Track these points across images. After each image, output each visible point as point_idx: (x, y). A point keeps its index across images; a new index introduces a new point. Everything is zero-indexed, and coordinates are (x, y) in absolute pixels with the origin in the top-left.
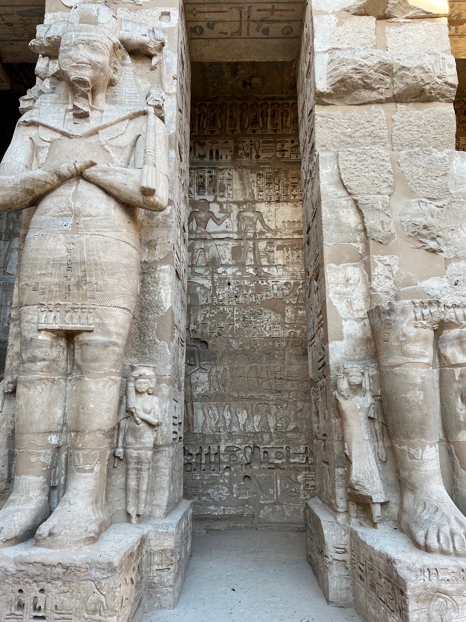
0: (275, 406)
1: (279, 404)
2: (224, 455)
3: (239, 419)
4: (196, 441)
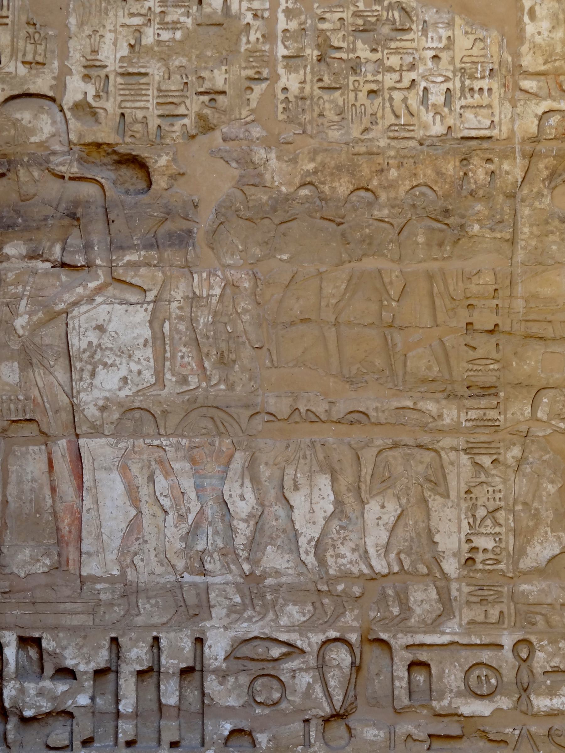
0: (464, 459)
1: (487, 447)
2: (223, 676)
3: (297, 515)
4: (93, 613)
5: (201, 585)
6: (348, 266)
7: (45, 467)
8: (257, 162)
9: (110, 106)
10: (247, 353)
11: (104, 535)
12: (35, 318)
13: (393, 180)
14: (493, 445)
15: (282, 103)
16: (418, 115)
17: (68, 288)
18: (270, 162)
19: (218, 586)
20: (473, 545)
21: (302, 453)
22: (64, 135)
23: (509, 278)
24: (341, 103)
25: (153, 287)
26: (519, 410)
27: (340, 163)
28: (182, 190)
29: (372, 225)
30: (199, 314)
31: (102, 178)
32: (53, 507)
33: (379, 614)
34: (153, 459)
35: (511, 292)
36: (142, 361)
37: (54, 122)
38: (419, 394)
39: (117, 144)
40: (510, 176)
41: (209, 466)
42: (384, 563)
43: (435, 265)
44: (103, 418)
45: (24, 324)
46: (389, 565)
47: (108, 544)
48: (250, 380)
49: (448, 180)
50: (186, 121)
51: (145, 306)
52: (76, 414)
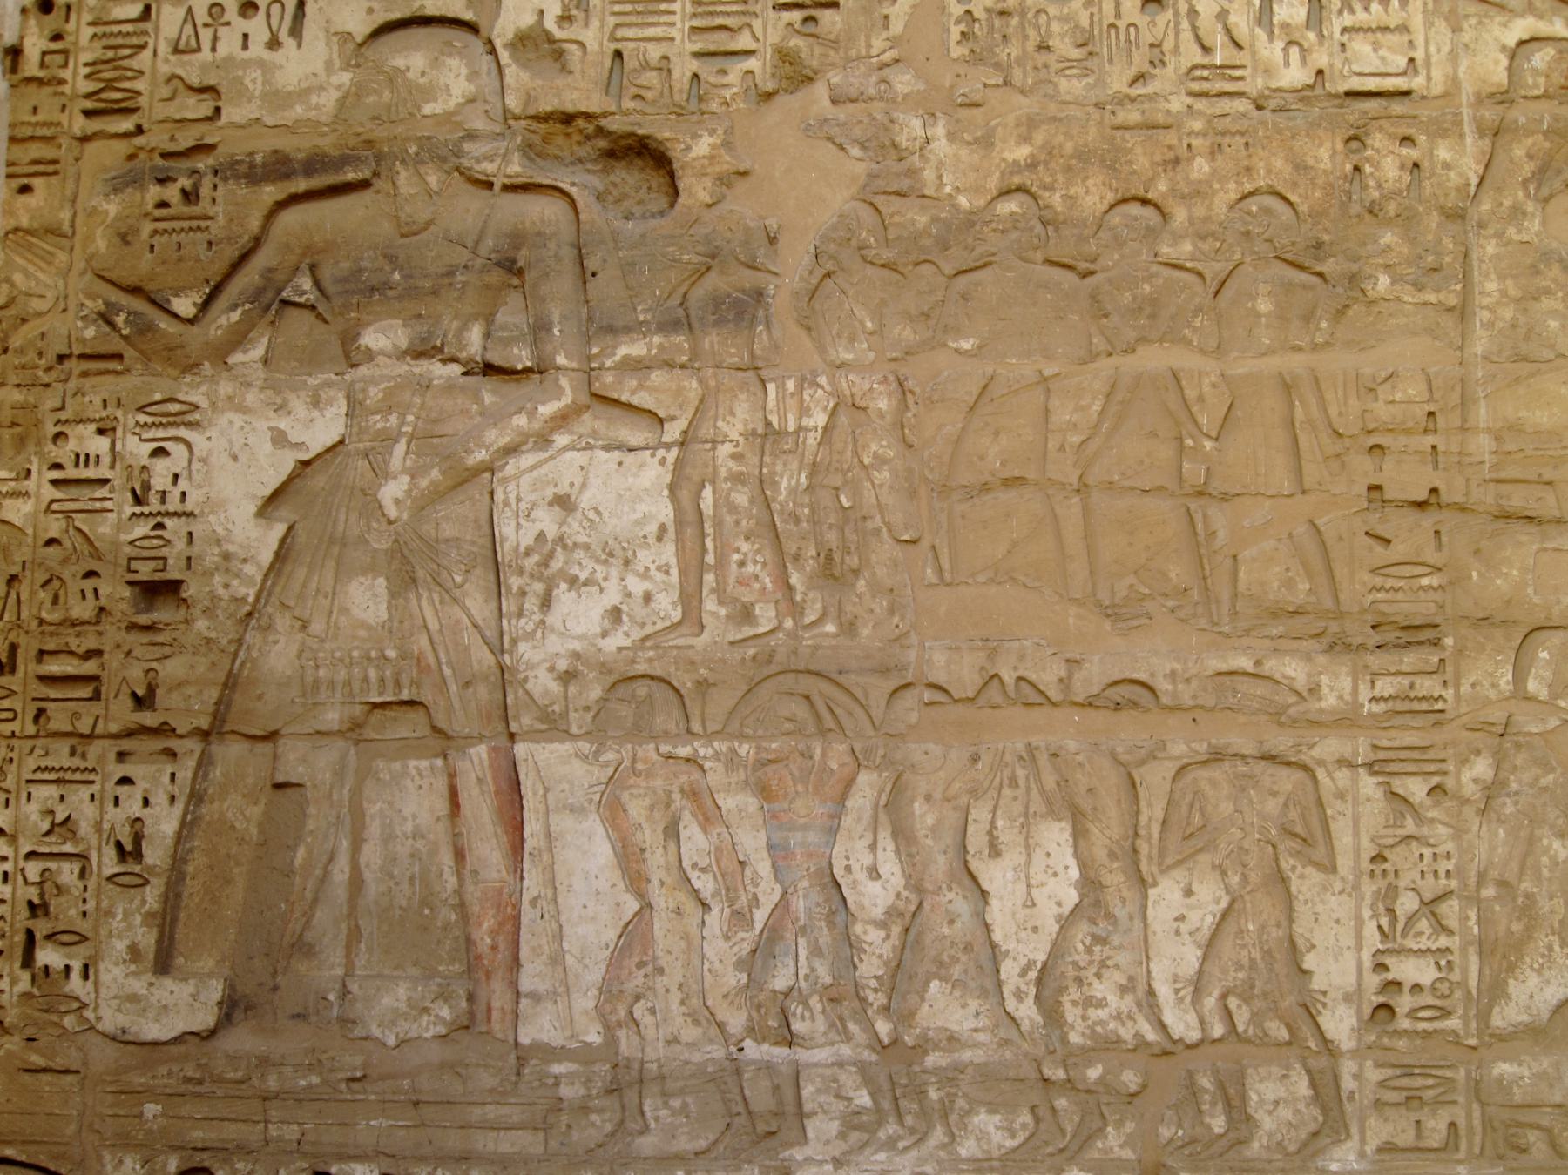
0: (1369, 785)
1: (1419, 758)
3: (997, 913)
4: (543, 1126)
5: (783, 1069)
6: (1105, 365)
7: (442, 807)
8: (904, 144)
9: (592, 36)
10: (884, 551)
11: (568, 957)
12: (424, 483)
13: (1200, 182)
14: (1430, 755)
15: (958, 22)
16: (1252, 45)
17: (496, 418)
18: (934, 145)
19: (820, 1070)
20: (1390, 976)
21: (1007, 773)
22: (495, 99)
23: (1458, 389)
24: (1085, 23)
25: (678, 413)
26: (1487, 676)
27: (1086, 145)
28: (743, 207)
29: (1156, 275)
30: (779, 468)
31: (573, 184)
32: (459, 892)
33: (1180, 1133)
34: (675, 789)
35: (1465, 420)
36: (653, 572)
37: (473, 75)
38: (1267, 642)
39: (605, 115)
40: (1452, 174)
41: (799, 804)
42: (1192, 1018)
43: (1296, 363)
44: (566, 698)
45: (400, 495)
46: (1202, 1022)
47: (577, 976)
48: (891, 612)
49: (1320, 181)
50: (752, 63)
51: (661, 453)
52: (509, 690)
